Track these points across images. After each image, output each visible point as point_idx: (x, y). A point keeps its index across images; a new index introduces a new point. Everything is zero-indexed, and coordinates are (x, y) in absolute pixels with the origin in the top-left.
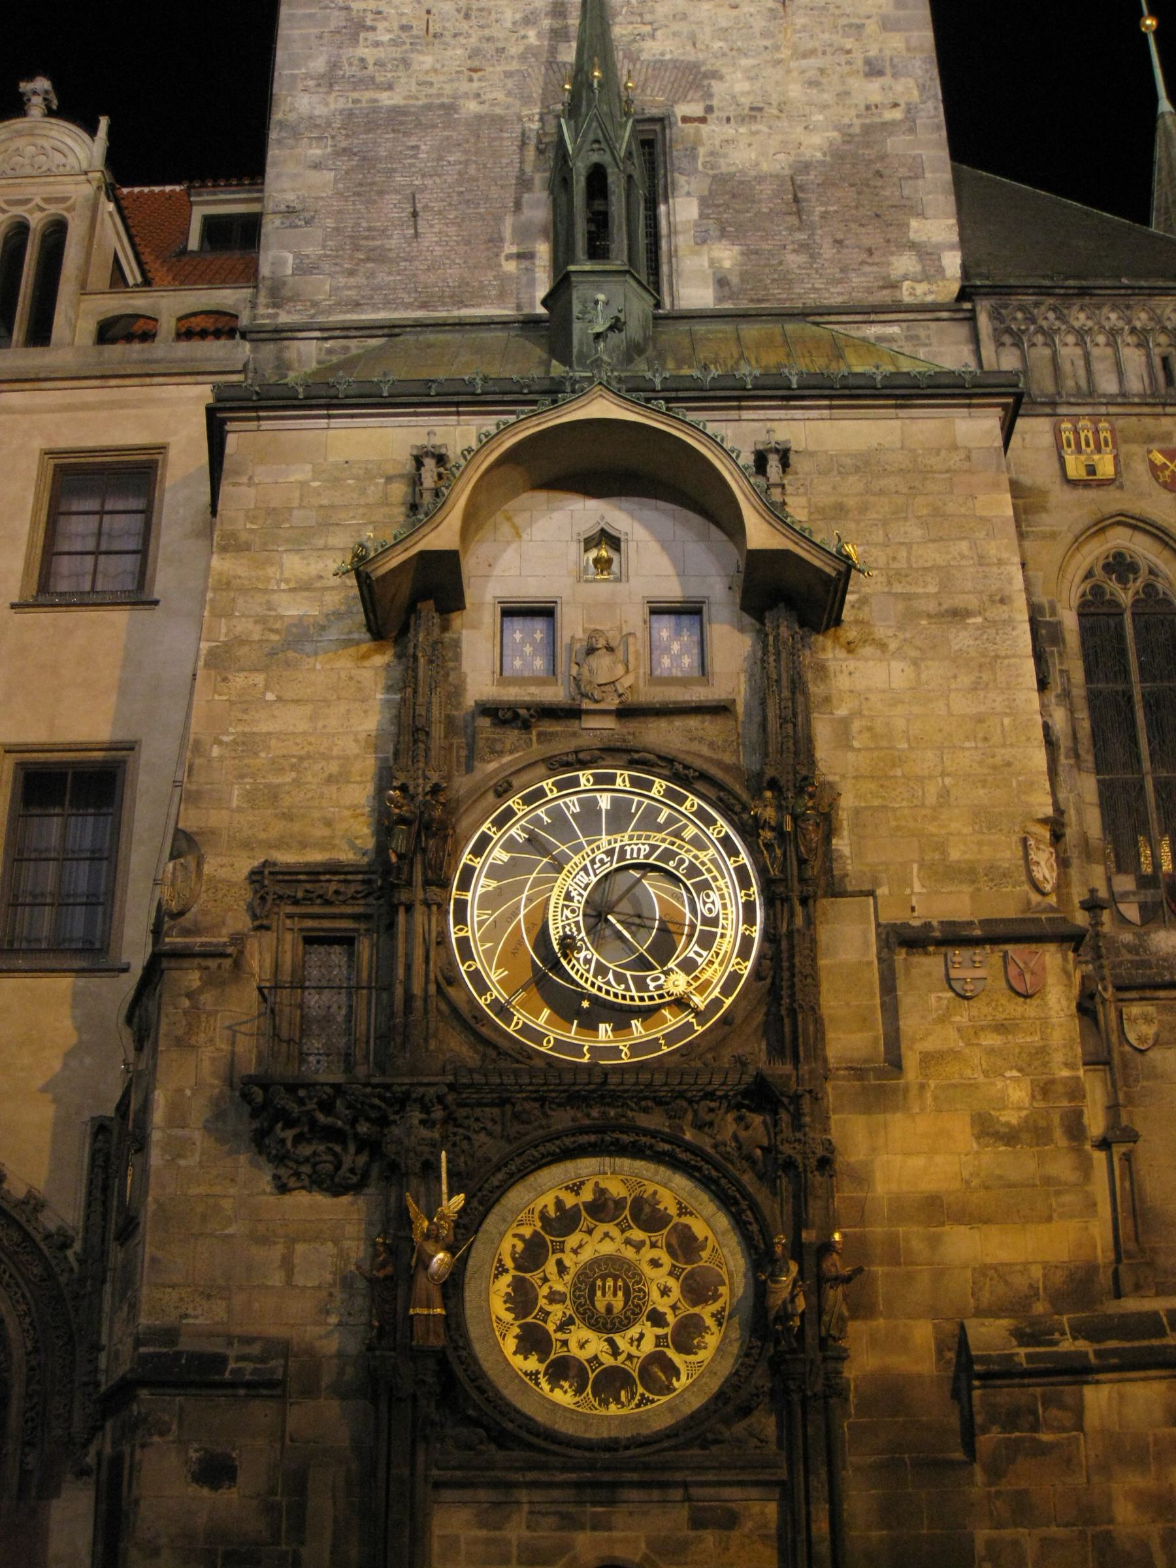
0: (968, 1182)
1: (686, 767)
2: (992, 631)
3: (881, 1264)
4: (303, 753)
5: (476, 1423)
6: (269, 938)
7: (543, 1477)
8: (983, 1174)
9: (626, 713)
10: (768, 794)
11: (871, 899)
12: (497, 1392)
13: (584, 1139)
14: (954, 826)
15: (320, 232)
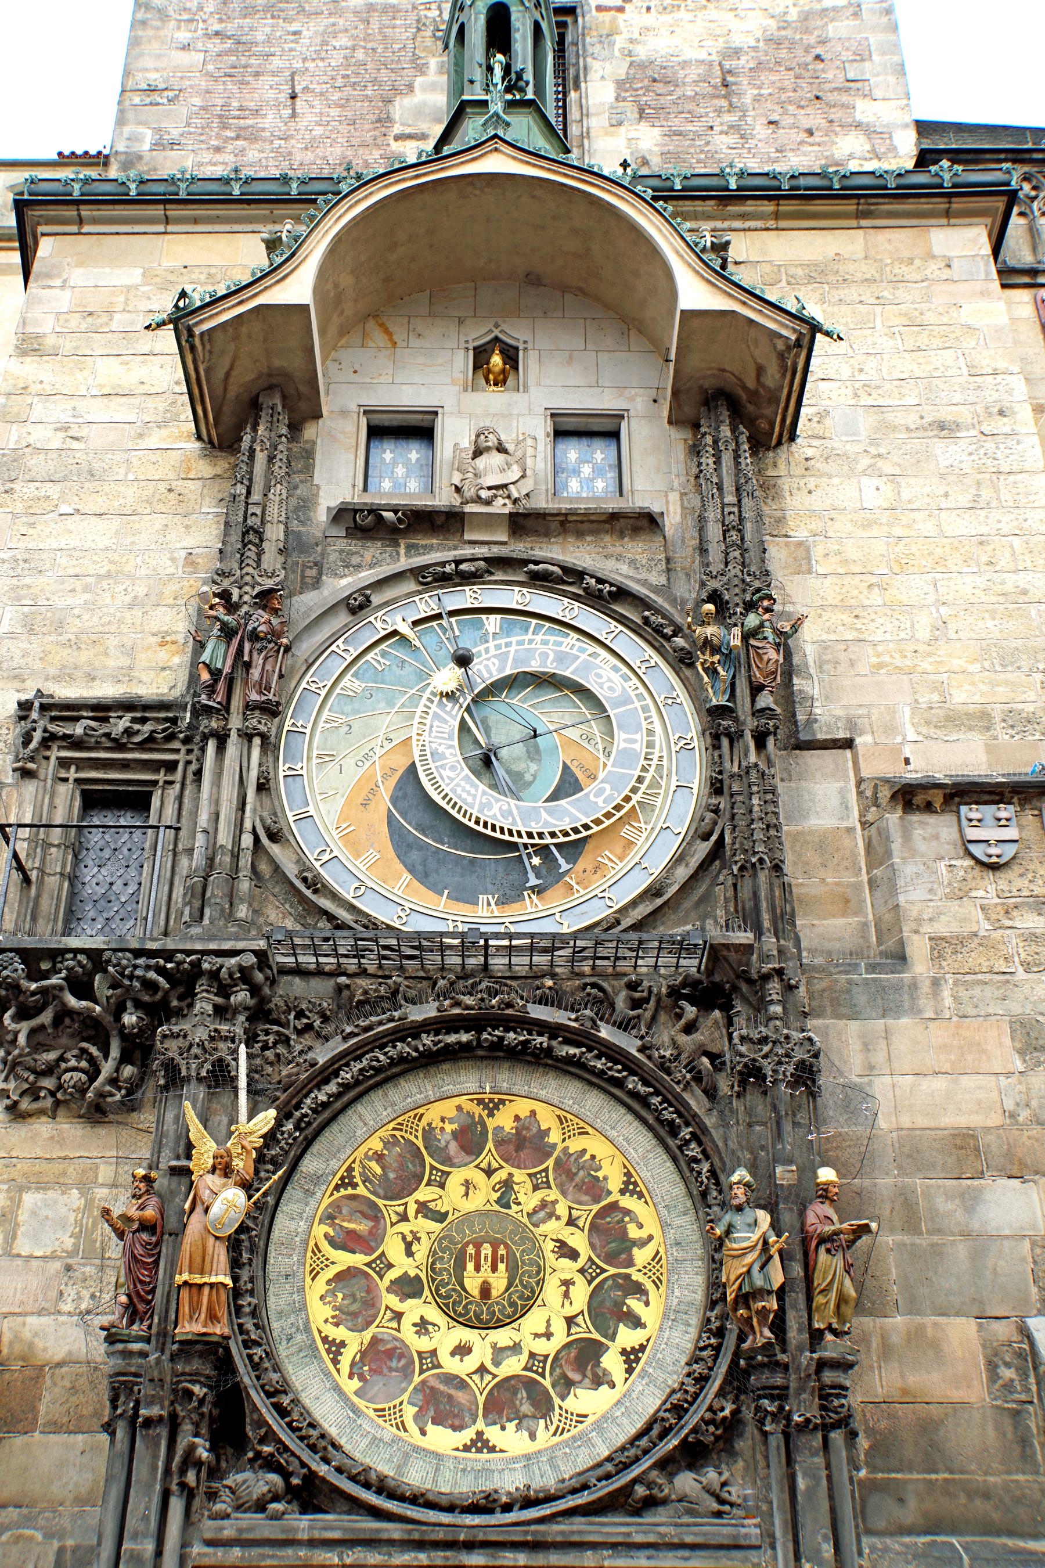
0: (1013, 1116)
1: (600, 581)
2: (990, 445)
3: (892, 1230)
4: (103, 571)
5: (270, 1464)
6: (30, 787)
7: (374, 1558)
8: (1034, 1103)
9: (524, 522)
10: (710, 607)
11: (848, 753)
12: (305, 1412)
13: (452, 1038)
14: (957, 663)
15: (184, 110)
